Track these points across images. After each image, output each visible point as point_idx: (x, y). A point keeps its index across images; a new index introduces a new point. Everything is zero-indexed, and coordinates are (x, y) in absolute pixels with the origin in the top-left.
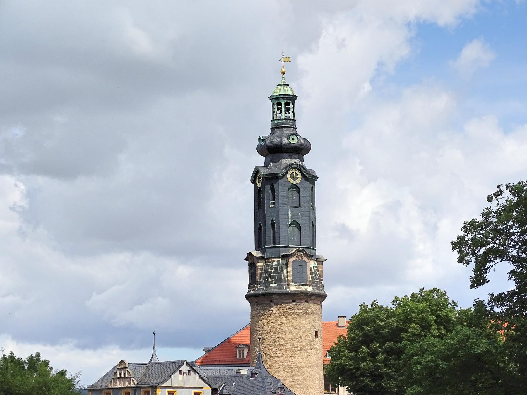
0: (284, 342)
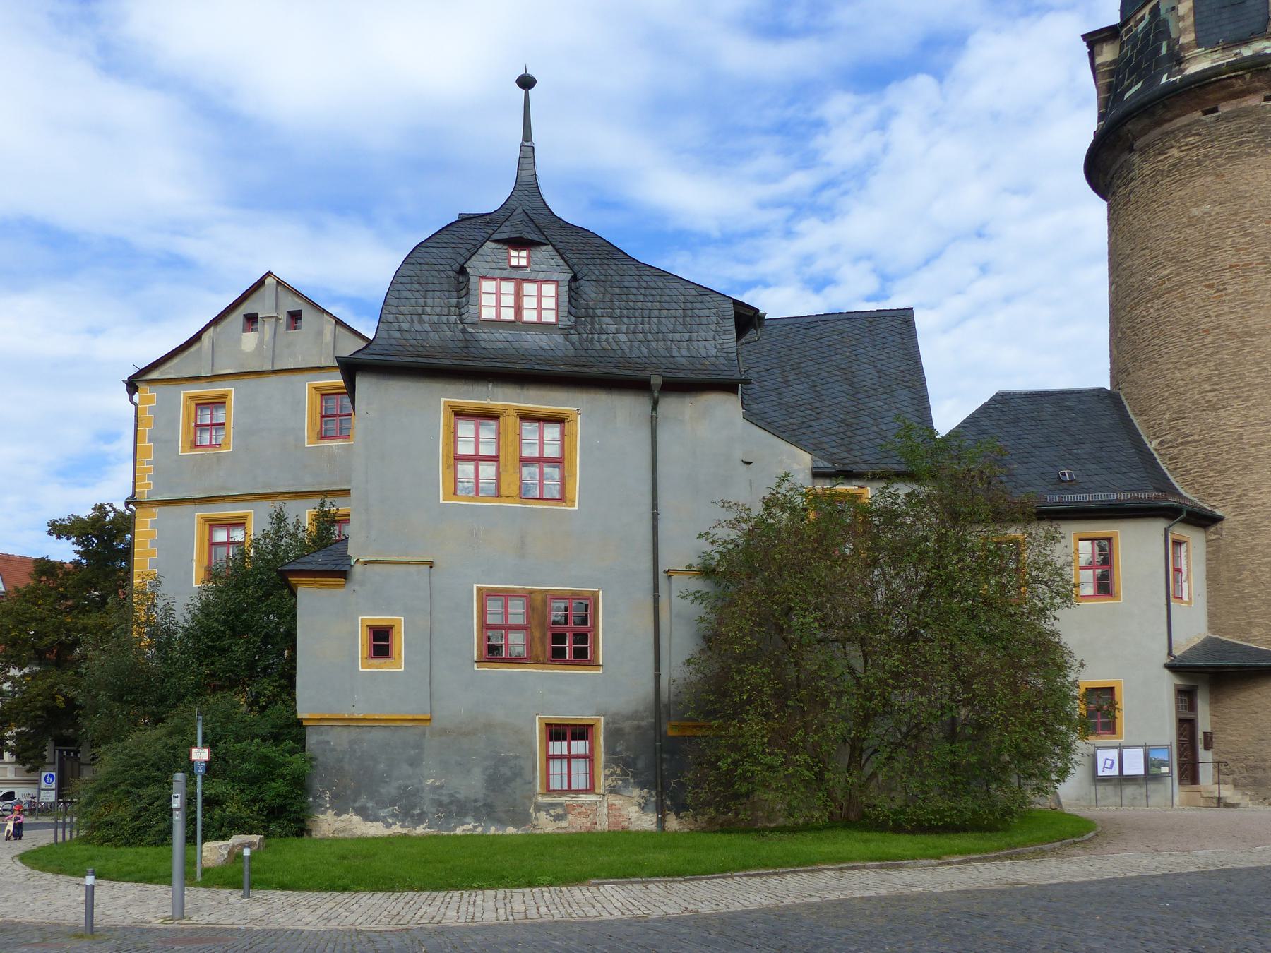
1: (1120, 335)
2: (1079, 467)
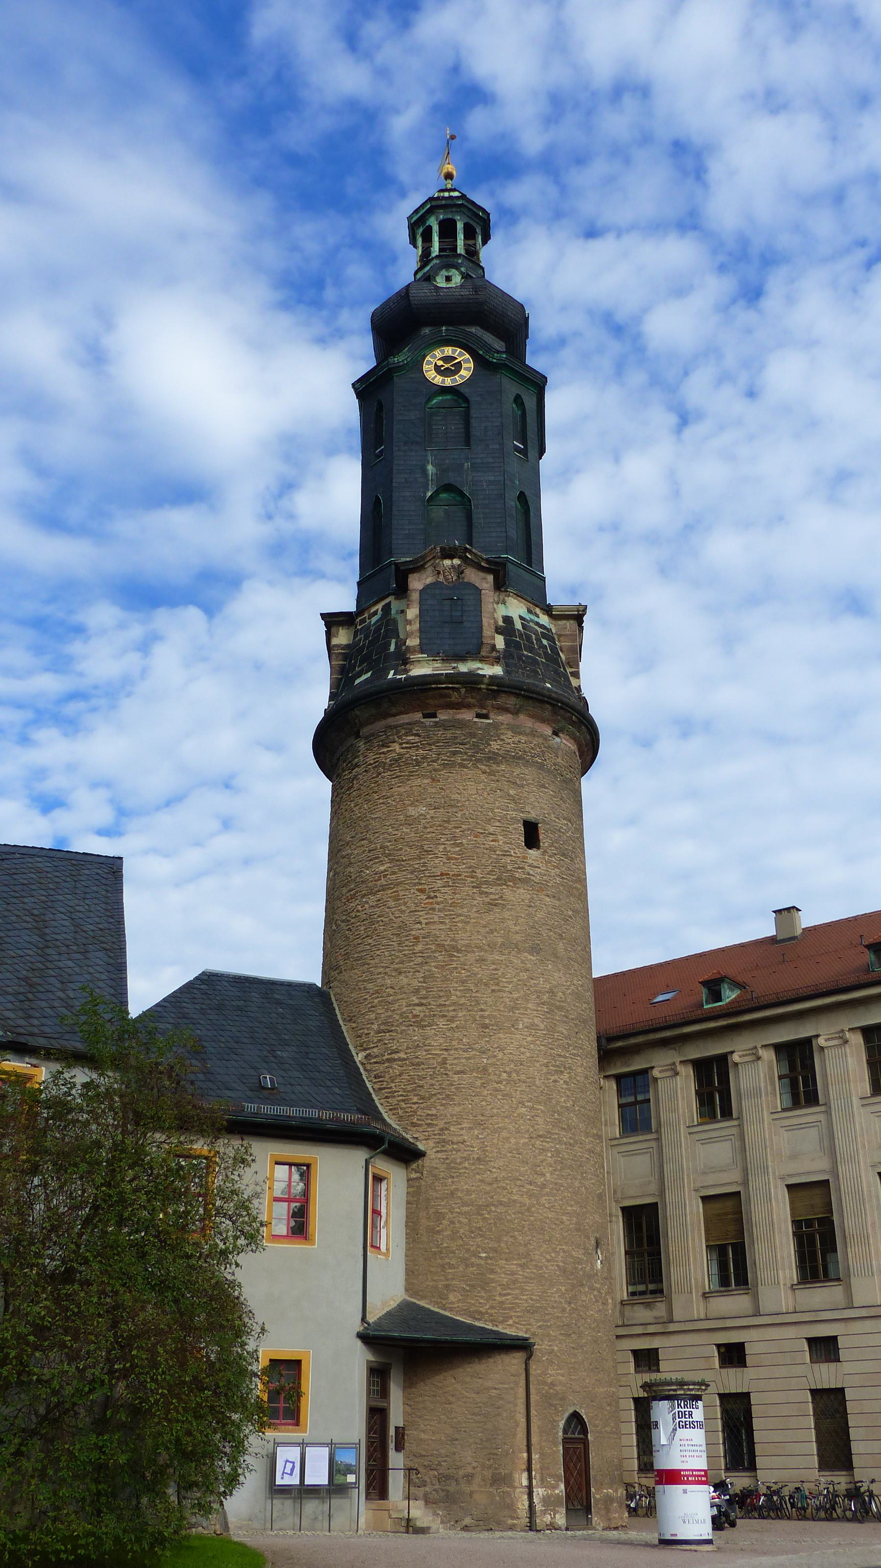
0: (391, 861)
1: (334, 927)
2: (284, 1074)
